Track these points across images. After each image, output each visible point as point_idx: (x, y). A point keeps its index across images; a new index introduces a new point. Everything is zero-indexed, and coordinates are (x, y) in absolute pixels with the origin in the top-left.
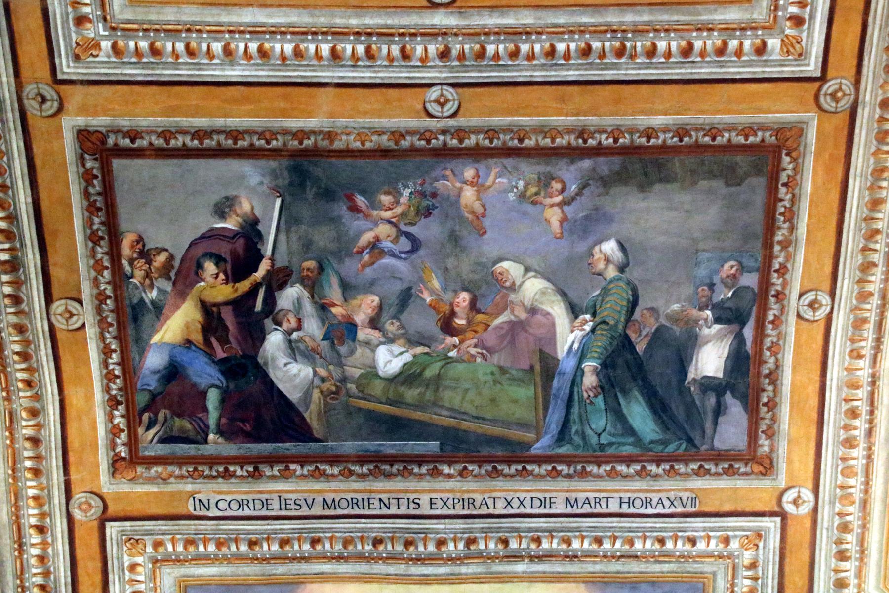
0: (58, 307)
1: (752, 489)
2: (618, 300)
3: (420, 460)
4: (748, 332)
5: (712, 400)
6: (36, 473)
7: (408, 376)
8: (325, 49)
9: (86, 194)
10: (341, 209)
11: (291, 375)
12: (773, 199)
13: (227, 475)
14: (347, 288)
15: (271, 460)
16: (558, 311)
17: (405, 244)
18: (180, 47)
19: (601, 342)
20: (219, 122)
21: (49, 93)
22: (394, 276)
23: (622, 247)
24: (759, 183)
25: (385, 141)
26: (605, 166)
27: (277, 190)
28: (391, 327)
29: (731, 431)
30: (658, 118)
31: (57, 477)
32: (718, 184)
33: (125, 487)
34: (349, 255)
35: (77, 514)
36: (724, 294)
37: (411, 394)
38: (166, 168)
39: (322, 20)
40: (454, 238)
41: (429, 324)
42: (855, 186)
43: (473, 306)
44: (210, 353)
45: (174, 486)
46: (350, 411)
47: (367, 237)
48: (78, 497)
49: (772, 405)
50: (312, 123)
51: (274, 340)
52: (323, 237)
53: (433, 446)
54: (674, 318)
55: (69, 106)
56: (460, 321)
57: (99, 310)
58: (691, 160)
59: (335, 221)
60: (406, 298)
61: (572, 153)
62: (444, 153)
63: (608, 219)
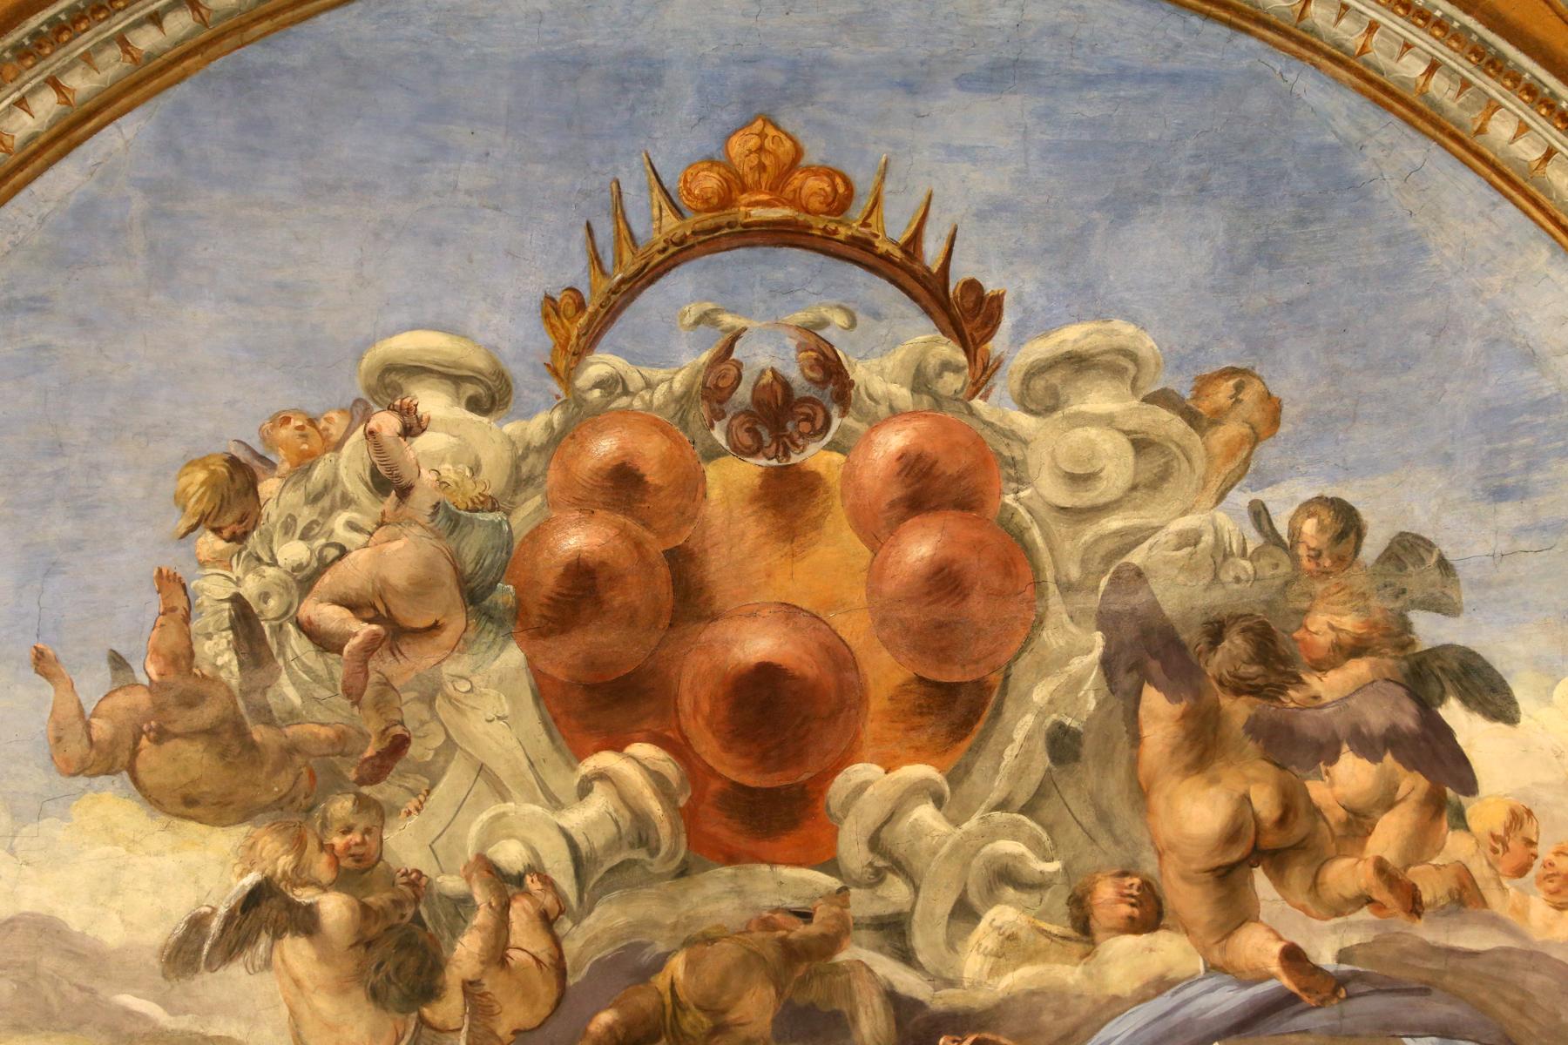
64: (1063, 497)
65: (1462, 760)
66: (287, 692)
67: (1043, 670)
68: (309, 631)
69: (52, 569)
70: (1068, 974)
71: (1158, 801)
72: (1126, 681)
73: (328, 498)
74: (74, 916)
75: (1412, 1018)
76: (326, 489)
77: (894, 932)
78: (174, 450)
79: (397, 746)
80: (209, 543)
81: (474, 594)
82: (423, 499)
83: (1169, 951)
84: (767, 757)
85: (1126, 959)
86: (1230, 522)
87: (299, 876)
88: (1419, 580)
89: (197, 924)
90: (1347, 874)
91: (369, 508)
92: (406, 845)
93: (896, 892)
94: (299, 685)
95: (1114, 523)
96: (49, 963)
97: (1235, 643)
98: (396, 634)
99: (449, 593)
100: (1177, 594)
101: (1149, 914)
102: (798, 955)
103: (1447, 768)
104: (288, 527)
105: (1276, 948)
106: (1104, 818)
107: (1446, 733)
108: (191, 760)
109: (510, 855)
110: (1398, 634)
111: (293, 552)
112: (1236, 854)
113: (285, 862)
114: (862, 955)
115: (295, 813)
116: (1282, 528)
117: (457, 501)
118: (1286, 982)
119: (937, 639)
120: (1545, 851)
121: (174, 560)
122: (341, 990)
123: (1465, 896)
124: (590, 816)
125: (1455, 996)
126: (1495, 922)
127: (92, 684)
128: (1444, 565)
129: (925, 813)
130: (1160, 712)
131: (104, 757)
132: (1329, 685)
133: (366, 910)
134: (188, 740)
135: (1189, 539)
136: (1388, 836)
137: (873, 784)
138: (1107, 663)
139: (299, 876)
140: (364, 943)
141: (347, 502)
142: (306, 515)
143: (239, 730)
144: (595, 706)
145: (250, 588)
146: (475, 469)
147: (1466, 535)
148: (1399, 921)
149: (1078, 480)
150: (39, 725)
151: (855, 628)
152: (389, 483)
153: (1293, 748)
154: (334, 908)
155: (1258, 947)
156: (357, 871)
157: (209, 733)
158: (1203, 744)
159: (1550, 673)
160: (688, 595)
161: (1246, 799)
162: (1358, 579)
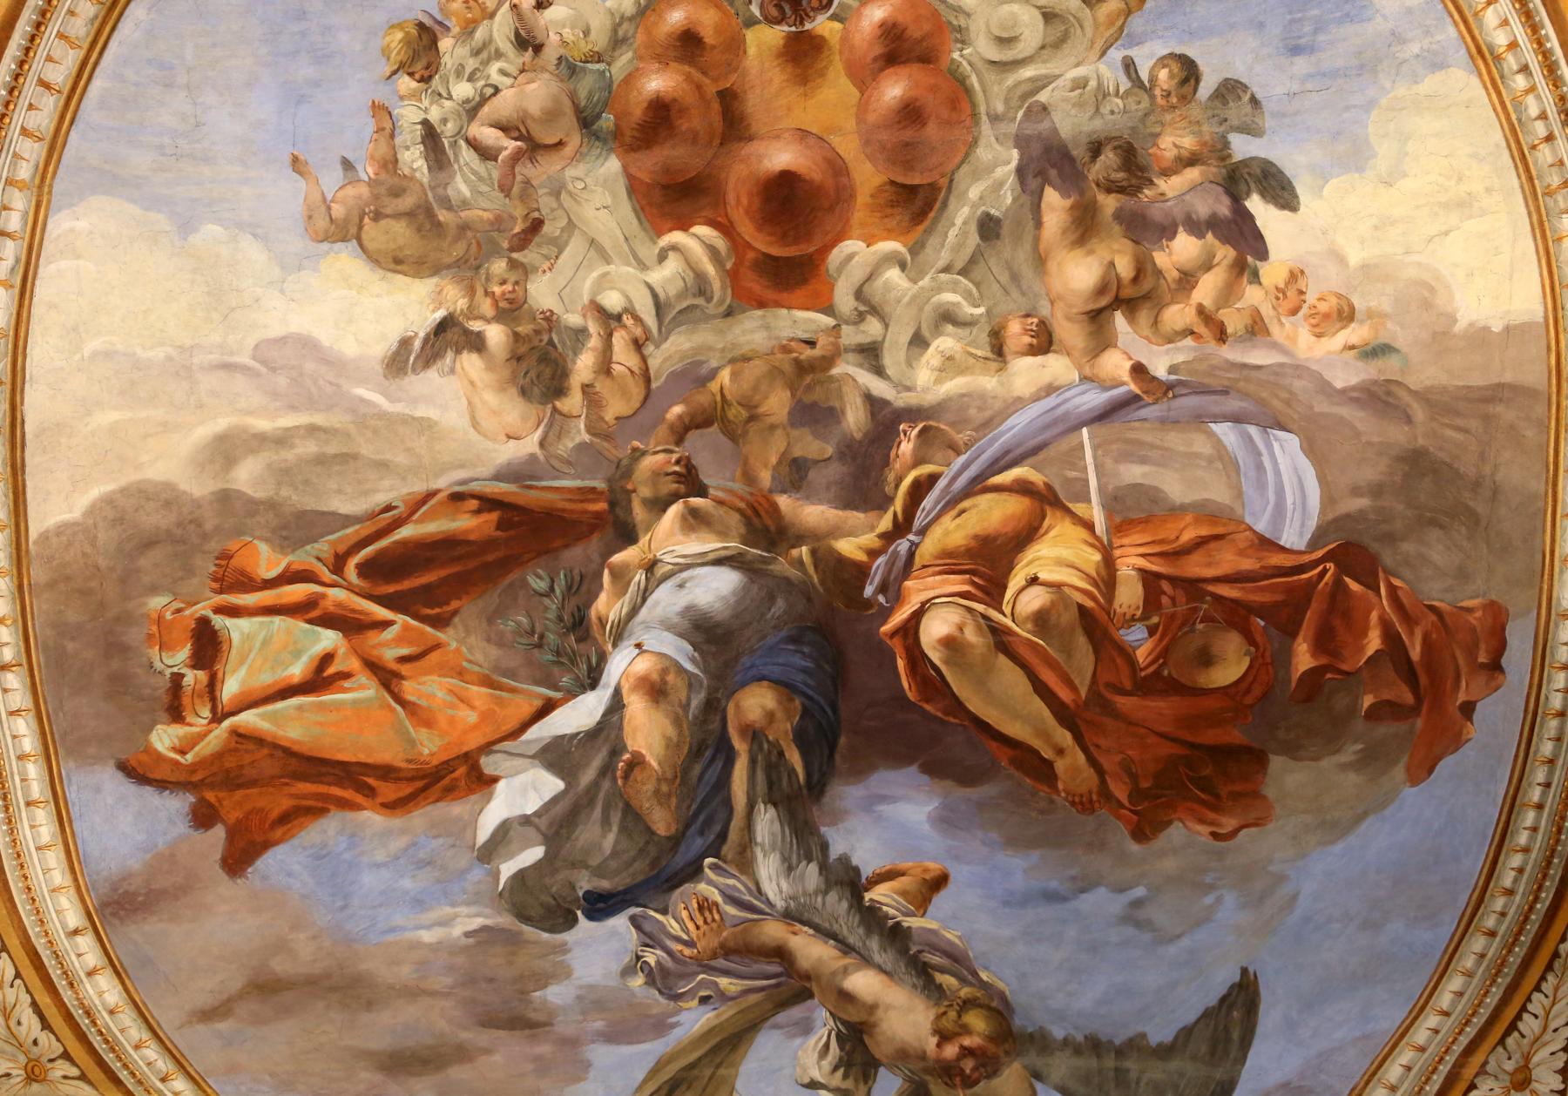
64: (994, 54)
65: (1259, 237)
66: (461, 187)
67: (976, 176)
68: (474, 144)
69: (301, 100)
70: (988, 382)
71: (1052, 266)
72: (1033, 184)
73: (488, 53)
74: (325, 336)
75: (1216, 409)
76: (485, 45)
77: (871, 354)
78: (380, 18)
79: (536, 226)
80: (406, 83)
81: (586, 122)
82: (550, 54)
83: (1056, 367)
84: (787, 235)
85: (1027, 373)
86: (1109, 71)
87: (471, 312)
88: (1237, 111)
89: (405, 343)
90: (1178, 315)
91: (515, 59)
92: (542, 293)
93: (873, 328)
94: (469, 182)
95: (1028, 72)
96: (310, 366)
97: (1109, 157)
98: (534, 148)
99: (569, 121)
100: (1071, 124)
101: (1043, 342)
102: (806, 371)
103: (1247, 241)
104: (459, 73)
105: (1128, 365)
106: (1015, 278)
107: (1248, 217)
108: (398, 233)
109: (612, 301)
110: (1220, 150)
111: (463, 90)
112: (1104, 302)
113: (462, 304)
114: (847, 368)
115: (468, 269)
116: (1144, 76)
117: (575, 55)
118: (1133, 387)
119: (904, 154)
120: (1311, 298)
121: (383, 94)
122: (502, 389)
123: (1256, 329)
124: (667, 275)
125: (1246, 395)
126: (1275, 346)
127: (331, 180)
128: (1254, 101)
129: (893, 274)
130: (1055, 204)
131: (343, 230)
132: (1171, 186)
133: (516, 335)
134: (397, 219)
135: (1080, 84)
136: (1206, 289)
137: (857, 255)
138: (1020, 171)
139: (471, 312)
140: (516, 358)
141: (499, 55)
142: (471, 63)
143: (430, 213)
144: (671, 199)
145: (434, 115)
146: (586, 33)
147: (1270, 79)
148: (1212, 346)
149: (1004, 41)
150: (297, 207)
151: (848, 146)
152: (527, 42)
153: (1145, 229)
154: (495, 335)
155: (1115, 364)
156: (510, 310)
157: (410, 215)
158: (1084, 226)
159: (1322, 176)
160: (733, 122)
161: (1112, 264)
162: (1195, 111)
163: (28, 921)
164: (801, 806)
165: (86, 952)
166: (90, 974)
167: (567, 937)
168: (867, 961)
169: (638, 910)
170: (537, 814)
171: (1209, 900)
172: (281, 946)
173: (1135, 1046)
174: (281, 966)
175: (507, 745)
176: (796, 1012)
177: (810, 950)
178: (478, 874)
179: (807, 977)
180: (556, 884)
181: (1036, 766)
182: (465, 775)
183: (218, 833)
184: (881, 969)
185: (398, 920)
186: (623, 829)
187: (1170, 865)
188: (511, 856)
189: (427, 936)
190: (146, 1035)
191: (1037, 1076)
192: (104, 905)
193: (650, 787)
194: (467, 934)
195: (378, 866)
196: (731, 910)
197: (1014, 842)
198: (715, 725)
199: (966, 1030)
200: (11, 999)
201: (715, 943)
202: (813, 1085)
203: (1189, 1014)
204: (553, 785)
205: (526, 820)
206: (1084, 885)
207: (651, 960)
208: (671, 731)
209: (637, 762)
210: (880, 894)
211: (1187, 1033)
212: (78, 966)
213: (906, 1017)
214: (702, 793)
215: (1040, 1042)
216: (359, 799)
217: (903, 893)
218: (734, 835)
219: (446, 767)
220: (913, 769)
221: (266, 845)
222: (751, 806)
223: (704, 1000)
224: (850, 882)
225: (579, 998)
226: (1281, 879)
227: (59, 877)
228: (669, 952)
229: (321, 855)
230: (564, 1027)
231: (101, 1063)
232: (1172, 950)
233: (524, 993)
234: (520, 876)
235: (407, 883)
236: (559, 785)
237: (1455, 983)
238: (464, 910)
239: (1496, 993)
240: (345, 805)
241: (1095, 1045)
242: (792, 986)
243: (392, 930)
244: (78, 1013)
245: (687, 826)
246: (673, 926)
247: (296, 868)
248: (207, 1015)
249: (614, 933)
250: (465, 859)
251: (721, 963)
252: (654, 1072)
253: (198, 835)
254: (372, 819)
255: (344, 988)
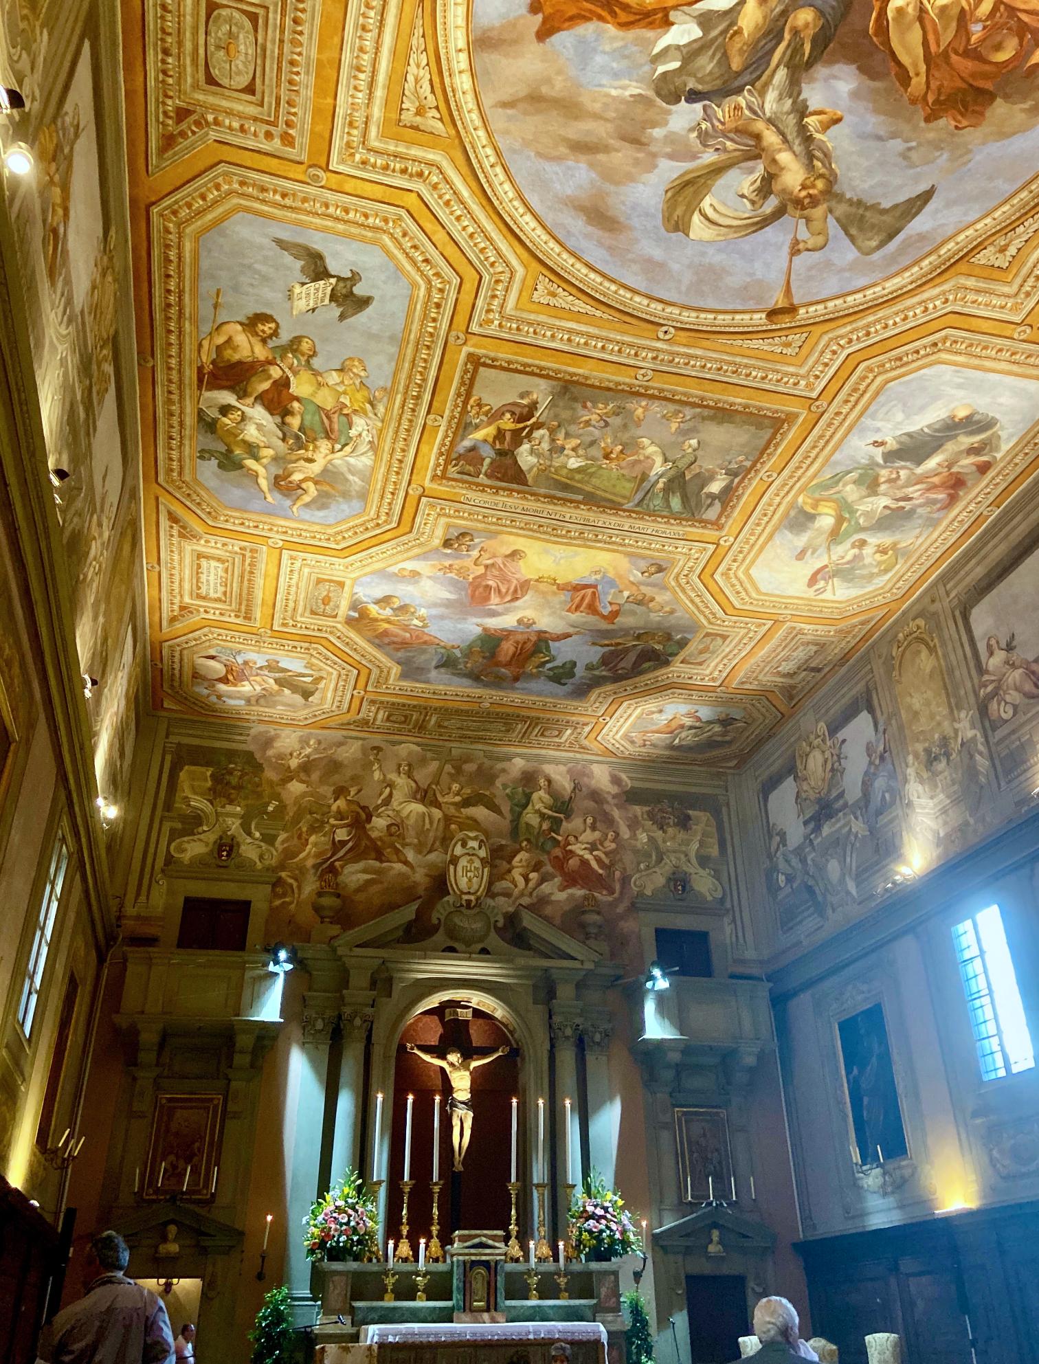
0: (431, 417)
1: (711, 534)
2: (687, 461)
3: (571, 501)
4: (736, 480)
5: (709, 501)
6: (398, 473)
7: (579, 470)
8: (600, 345)
9: (462, 377)
10: (579, 406)
11: (526, 457)
12: (773, 436)
13: (483, 491)
14: (567, 435)
15: (504, 489)
16: (659, 460)
17: (602, 423)
18: (531, 330)
19: (672, 472)
20: (537, 362)
21: (462, 336)
22: (591, 434)
23: (699, 443)
24: (767, 434)
25: (611, 385)
26: (706, 412)
27: (552, 393)
28: (581, 452)
29: (712, 514)
30: (738, 400)
31: (406, 477)
32: (753, 429)
33: (435, 486)
34: (574, 423)
35: (411, 492)
36: (734, 466)
37: (578, 477)
38: (504, 375)
39: (604, 334)
40: (625, 426)
41: (599, 454)
42: (809, 440)
43: (621, 452)
44: (493, 446)
45: (457, 490)
46: (548, 478)
47: (586, 418)
48: (413, 486)
49: (733, 507)
50: (581, 371)
51: (526, 447)
52: (566, 414)
53: (580, 497)
54: (708, 470)
55: (469, 343)
56: (613, 456)
57: (450, 422)
58: (744, 418)
59: (574, 409)
60: (593, 443)
61: (694, 405)
62: (638, 394)
63: (698, 432)
163: (440, 39)
164: (799, 69)
165: (461, 62)
166: (460, 72)
167: (673, 108)
168: (791, 149)
169: (707, 102)
170: (684, 46)
171: (938, 154)
172: (548, 81)
173: (874, 208)
174: (545, 90)
175: (685, 8)
176: (751, 164)
177: (771, 138)
178: (647, 68)
179: (763, 150)
180: (678, 82)
181: (904, 78)
182: (661, 19)
183: (540, 17)
184: (794, 152)
185: (604, 82)
186: (719, 62)
187: (931, 135)
188: (664, 63)
189: (614, 92)
190: (475, 107)
191: (831, 211)
192: (476, 41)
193: (739, 45)
194: (631, 96)
195: (604, 52)
196: (747, 112)
197: (876, 111)
198: (780, 24)
199: (813, 186)
200: (421, 74)
201: (733, 125)
202: (743, 196)
203: (902, 198)
204: (698, 33)
205: (678, 47)
206: (894, 136)
207: (704, 127)
208: (760, 21)
209: (739, 32)
210: (811, 121)
211: (896, 206)
212: (456, 67)
213: (793, 175)
214: (760, 54)
215: (840, 197)
216: (609, 18)
217: (820, 122)
218: (764, 78)
219: (654, 12)
220: (854, 67)
221: (559, 30)
222: (778, 66)
223: (717, 150)
224: (801, 111)
225: (666, 136)
226: (969, 151)
227: (461, 21)
228: (713, 126)
229: (582, 41)
230: (653, 148)
231: (451, 115)
232: (911, 171)
233: (644, 128)
234: (665, 74)
235: (614, 65)
236: (700, 34)
237: (1006, 208)
238: (634, 84)
239: (1018, 215)
240: (601, 18)
241: (859, 203)
242: (755, 150)
243: (600, 85)
244: (449, 90)
245: (746, 69)
246: (720, 114)
247: (569, 45)
248: (505, 105)
249: (694, 111)
250: (643, 59)
251: (732, 135)
252: (681, 176)
253: (530, 17)
254: (610, 29)
255: (569, 107)
